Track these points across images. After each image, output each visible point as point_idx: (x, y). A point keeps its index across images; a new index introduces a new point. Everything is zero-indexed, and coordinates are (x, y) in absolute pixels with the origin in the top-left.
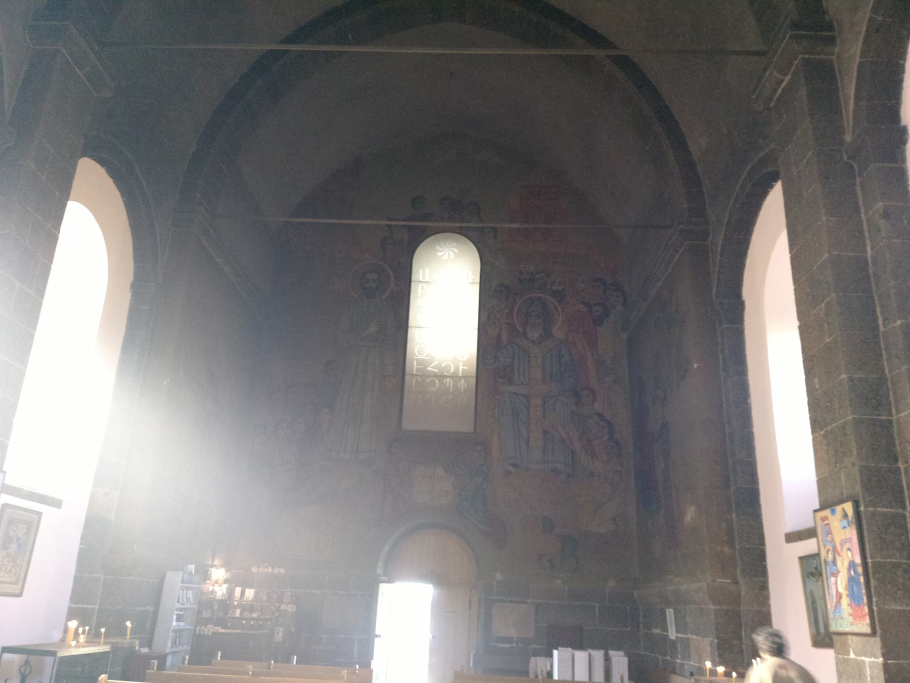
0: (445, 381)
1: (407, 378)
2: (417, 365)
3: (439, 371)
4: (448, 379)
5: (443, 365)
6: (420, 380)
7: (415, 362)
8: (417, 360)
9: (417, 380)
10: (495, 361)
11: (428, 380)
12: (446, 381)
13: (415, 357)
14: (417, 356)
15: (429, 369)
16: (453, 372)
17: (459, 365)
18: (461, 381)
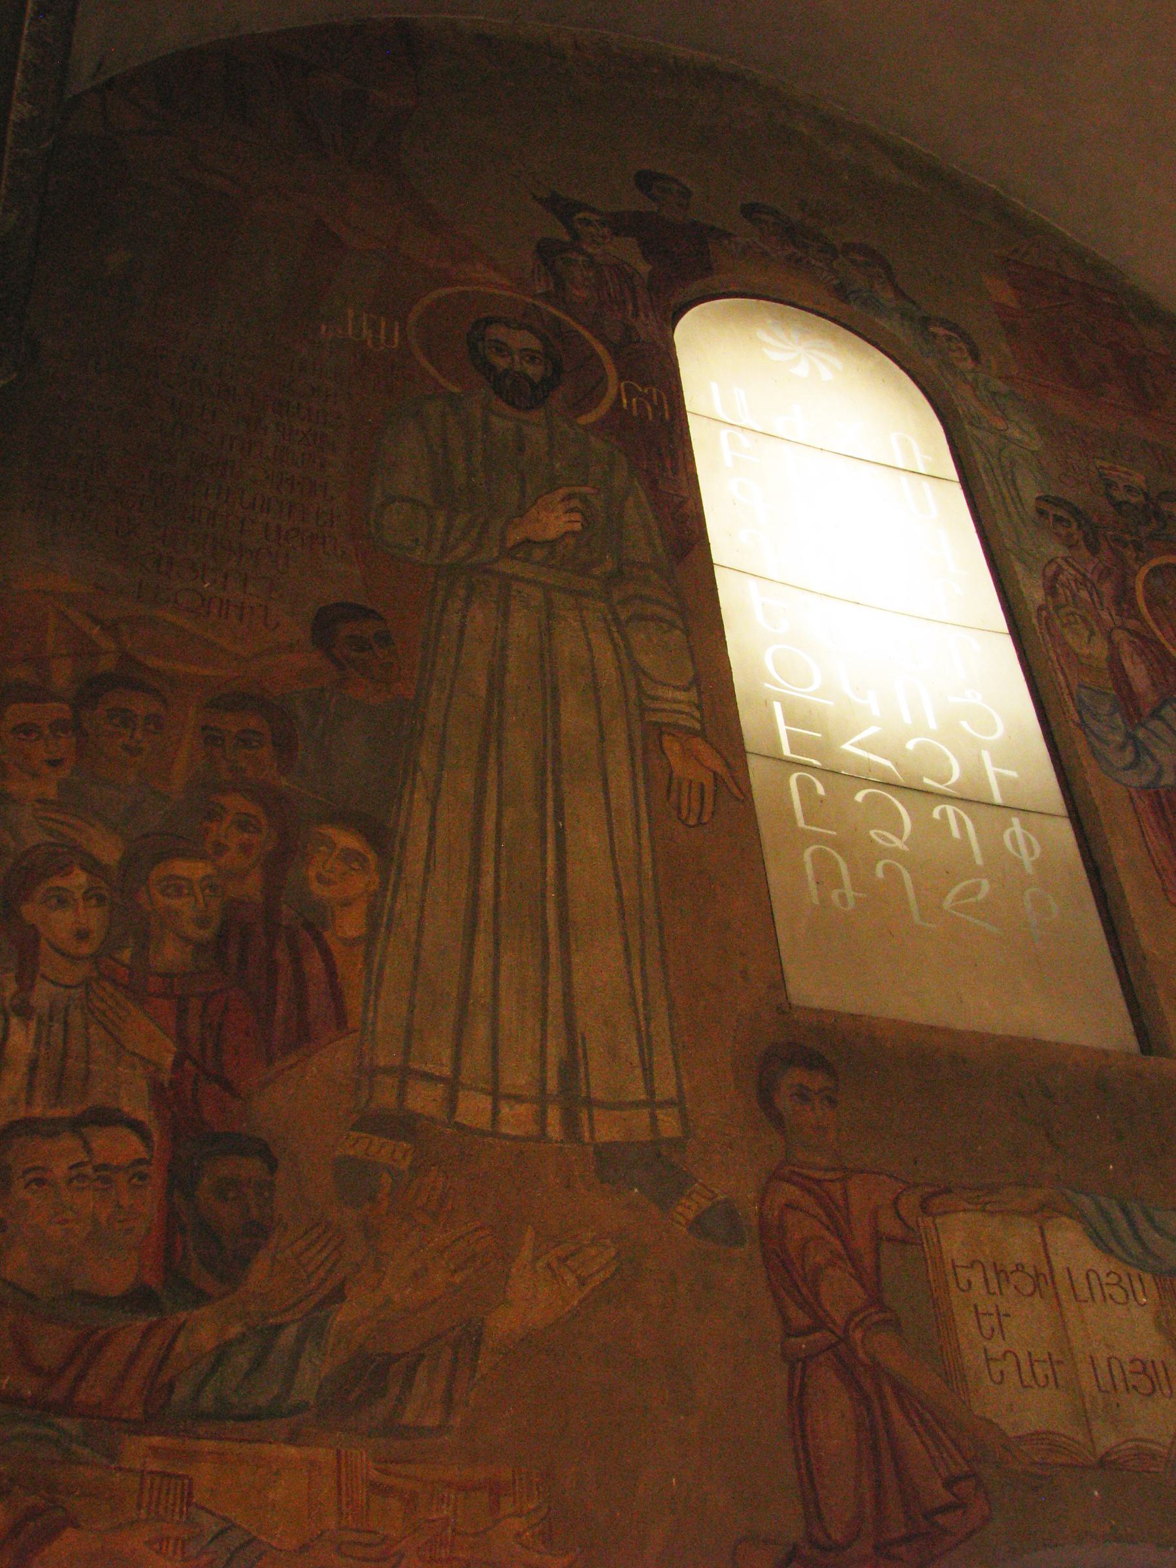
0: (936, 814)
1: (757, 770)
2: (788, 721)
3: (896, 765)
4: (950, 809)
5: (910, 745)
6: (821, 790)
7: (777, 708)
8: (781, 699)
9: (806, 788)
10: (1137, 755)
11: (859, 797)
12: (943, 813)
13: (767, 685)
14: (776, 684)
15: (847, 747)
16: (957, 783)
17: (979, 757)
18: (1011, 825)
